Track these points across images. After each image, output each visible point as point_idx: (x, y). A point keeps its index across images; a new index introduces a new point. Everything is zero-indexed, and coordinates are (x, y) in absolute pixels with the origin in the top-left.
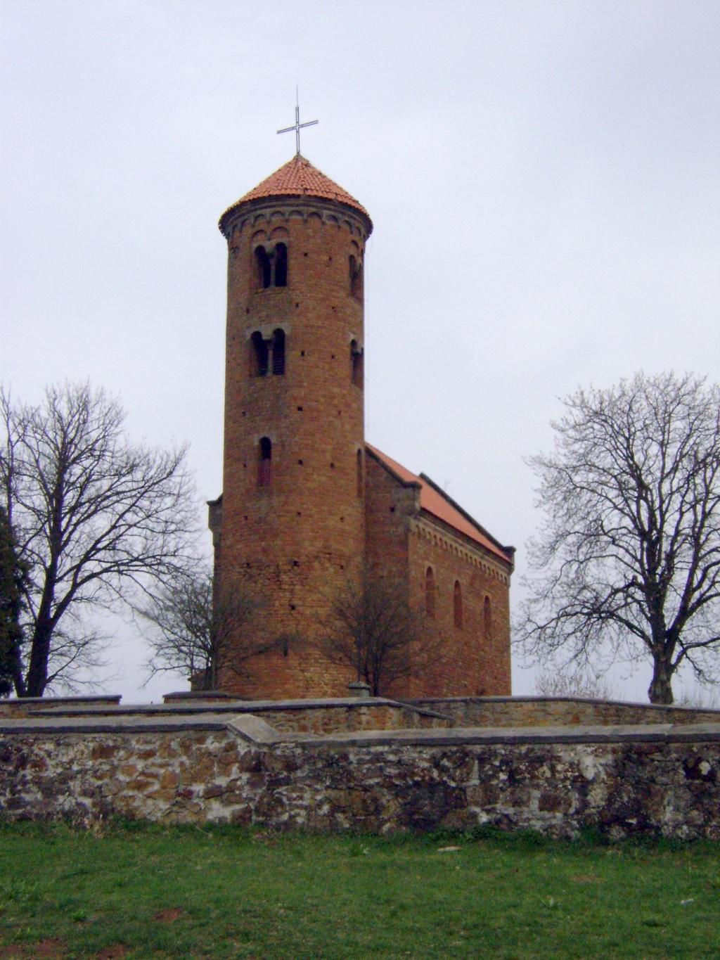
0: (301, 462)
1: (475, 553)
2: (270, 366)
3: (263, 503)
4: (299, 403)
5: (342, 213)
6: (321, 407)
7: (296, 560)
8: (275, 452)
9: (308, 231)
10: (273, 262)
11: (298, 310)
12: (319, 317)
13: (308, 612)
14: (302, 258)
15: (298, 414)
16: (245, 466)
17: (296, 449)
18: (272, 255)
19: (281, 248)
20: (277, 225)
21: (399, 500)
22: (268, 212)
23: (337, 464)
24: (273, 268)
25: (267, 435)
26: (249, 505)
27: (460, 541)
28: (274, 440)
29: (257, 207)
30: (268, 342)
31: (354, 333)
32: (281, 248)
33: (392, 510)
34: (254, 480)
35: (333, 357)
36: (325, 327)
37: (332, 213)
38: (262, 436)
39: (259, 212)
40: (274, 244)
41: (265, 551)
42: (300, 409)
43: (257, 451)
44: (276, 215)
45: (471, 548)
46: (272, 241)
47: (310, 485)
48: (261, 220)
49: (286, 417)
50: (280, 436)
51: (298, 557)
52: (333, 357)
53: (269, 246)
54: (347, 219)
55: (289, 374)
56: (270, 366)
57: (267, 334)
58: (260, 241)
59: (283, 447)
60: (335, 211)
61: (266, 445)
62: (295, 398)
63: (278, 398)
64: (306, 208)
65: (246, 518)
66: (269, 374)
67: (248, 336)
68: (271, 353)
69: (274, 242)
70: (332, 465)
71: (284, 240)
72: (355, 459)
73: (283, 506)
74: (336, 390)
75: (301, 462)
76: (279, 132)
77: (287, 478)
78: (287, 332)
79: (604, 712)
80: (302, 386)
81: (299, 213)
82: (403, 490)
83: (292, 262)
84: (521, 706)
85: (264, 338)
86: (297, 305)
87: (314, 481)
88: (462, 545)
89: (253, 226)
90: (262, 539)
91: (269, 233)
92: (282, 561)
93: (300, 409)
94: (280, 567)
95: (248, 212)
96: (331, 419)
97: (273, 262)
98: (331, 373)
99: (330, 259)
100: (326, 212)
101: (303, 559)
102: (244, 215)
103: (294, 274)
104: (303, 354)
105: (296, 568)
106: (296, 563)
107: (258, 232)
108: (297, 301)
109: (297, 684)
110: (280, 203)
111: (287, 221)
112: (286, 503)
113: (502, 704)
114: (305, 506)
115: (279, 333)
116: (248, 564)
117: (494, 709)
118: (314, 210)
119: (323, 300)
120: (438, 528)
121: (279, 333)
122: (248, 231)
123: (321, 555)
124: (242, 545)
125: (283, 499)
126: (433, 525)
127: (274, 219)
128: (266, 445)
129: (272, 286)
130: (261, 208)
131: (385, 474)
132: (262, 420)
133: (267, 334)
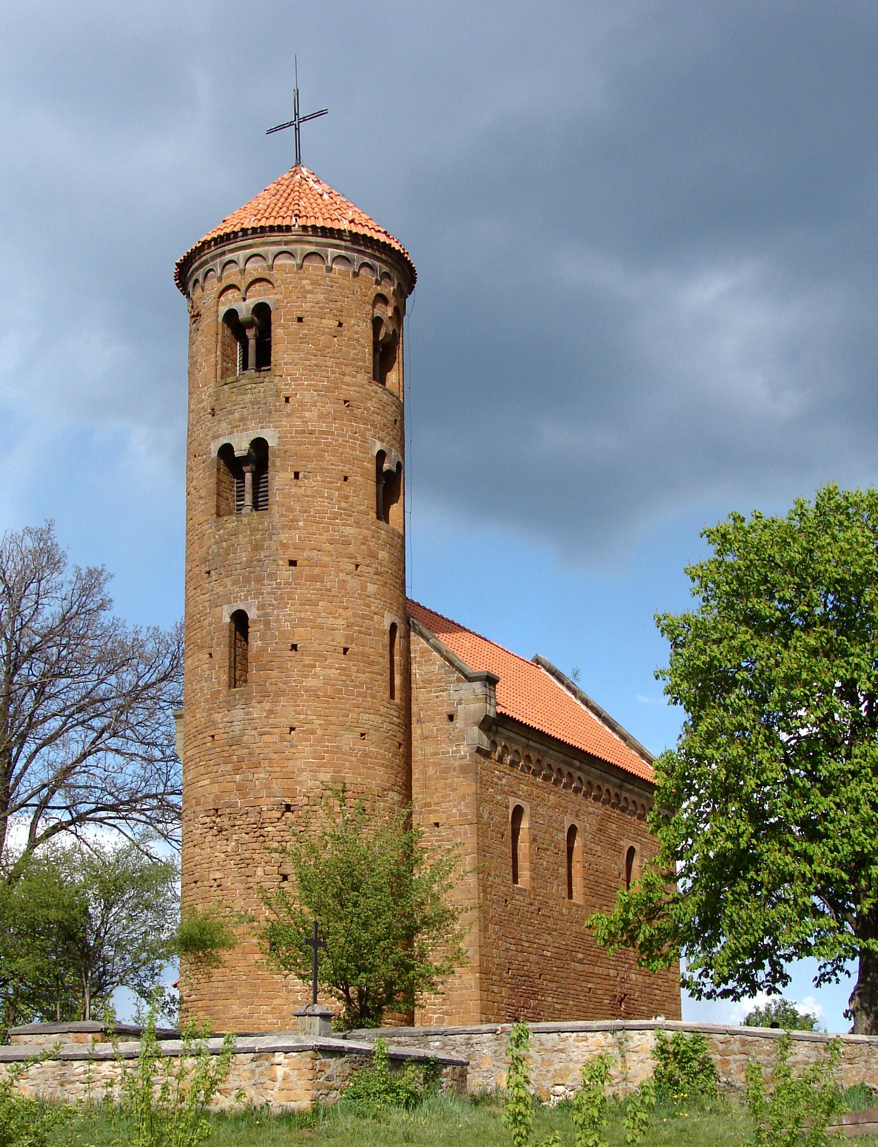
0: (294, 647)
1: (608, 782)
3: (238, 713)
4: (292, 554)
5: (358, 251)
6: (325, 559)
7: (288, 801)
8: (254, 631)
9: (304, 282)
10: (250, 333)
11: (289, 408)
12: (322, 417)
14: (295, 325)
15: (286, 573)
17: (287, 626)
18: (249, 324)
19: (262, 310)
20: (256, 275)
21: (459, 703)
22: (241, 255)
23: (353, 648)
24: (252, 342)
25: (242, 607)
26: (217, 717)
27: (577, 763)
28: (252, 614)
29: (226, 248)
31: (382, 441)
32: (262, 310)
33: (451, 718)
34: (225, 677)
35: (346, 479)
36: (332, 434)
37: (343, 252)
39: (228, 257)
40: (252, 306)
41: (241, 789)
42: (293, 563)
43: (227, 633)
45: (598, 772)
47: (310, 682)
48: (232, 269)
49: (272, 576)
50: (261, 607)
52: (346, 479)
53: (245, 310)
54: (367, 260)
55: (275, 509)
56: (248, 498)
57: (241, 447)
58: (231, 300)
59: (267, 623)
60: (346, 248)
61: (240, 620)
62: (284, 546)
63: (257, 547)
64: (298, 247)
66: (246, 510)
68: (248, 477)
69: (252, 302)
70: (346, 650)
72: (387, 640)
74: (349, 530)
75: (294, 647)
76: (270, 132)
77: (274, 673)
79: (721, 1047)
81: (291, 254)
82: (466, 685)
83: (278, 332)
84: (586, 1039)
85: (237, 454)
86: (287, 400)
87: (316, 676)
88: (580, 769)
89: (220, 279)
90: (237, 770)
91: (243, 289)
93: (293, 563)
95: (214, 258)
96: (342, 576)
97: (250, 333)
98: (344, 505)
99: (340, 325)
100: (331, 252)
101: (301, 800)
102: (206, 262)
103: (280, 351)
104: (297, 475)
105: (288, 814)
106: (288, 808)
108: (287, 394)
109: (292, 997)
111: (271, 268)
112: (271, 712)
113: (555, 1035)
114: (302, 717)
115: (259, 445)
117: (541, 1044)
118: (312, 249)
119: (328, 389)
120: (531, 743)
121: (259, 445)
122: (213, 286)
125: (267, 706)
126: (523, 740)
128: (240, 620)
129: (251, 372)
131: (440, 661)
132: (234, 583)
133: (241, 447)
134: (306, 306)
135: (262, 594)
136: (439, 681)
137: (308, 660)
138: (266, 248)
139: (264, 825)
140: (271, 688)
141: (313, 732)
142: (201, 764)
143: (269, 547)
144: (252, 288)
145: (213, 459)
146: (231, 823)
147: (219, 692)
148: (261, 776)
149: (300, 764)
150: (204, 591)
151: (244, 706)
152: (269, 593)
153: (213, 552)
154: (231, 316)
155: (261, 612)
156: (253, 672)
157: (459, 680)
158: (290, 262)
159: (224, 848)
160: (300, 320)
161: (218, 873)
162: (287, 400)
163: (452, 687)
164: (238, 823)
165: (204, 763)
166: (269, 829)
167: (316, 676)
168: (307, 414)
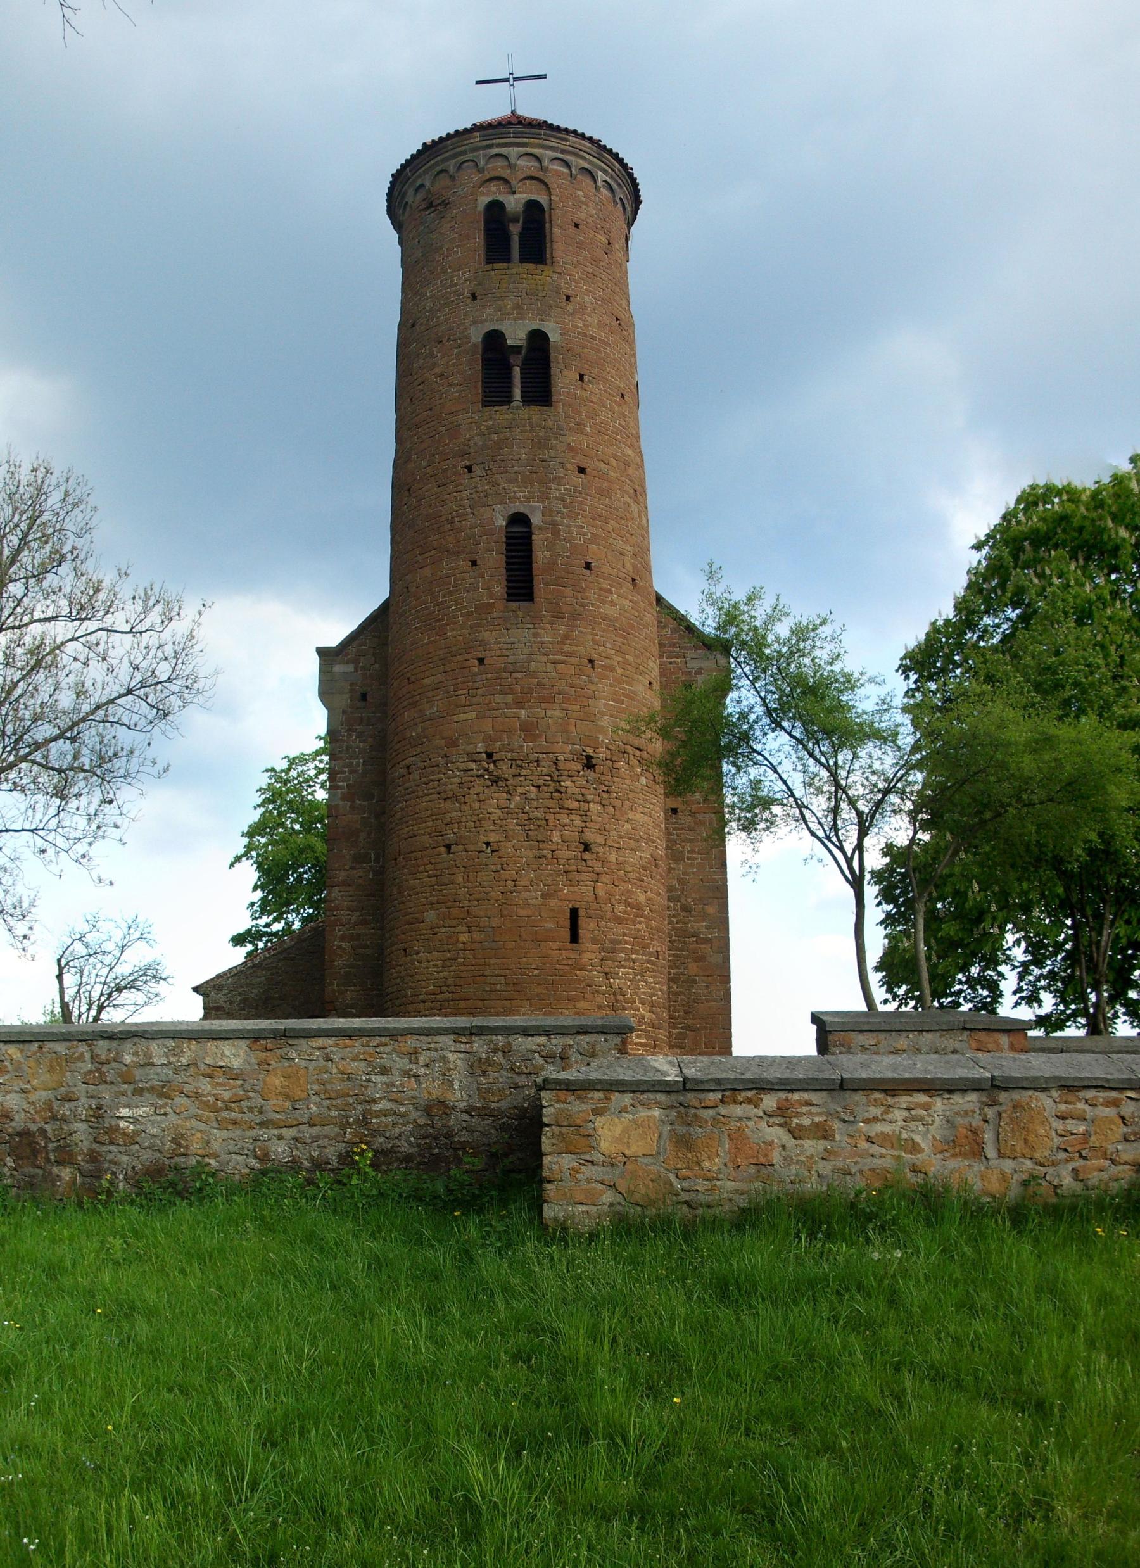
0: (588, 566)
2: (517, 393)
3: (521, 635)
7: (590, 751)
10: (515, 229)
11: (570, 307)
13: (613, 857)
14: (572, 229)
16: (474, 563)
20: (528, 173)
22: (512, 152)
24: (516, 239)
25: (522, 509)
28: (536, 519)
30: (517, 349)
32: (533, 207)
38: (513, 511)
39: (496, 151)
42: (582, 470)
44: (525, 158)
46: (517, 196)
49: (559, 480)
51: (595, 749)
53: (514, 202)
56: (517, 393)
57: (516, 334)
59: (556, 533)
63: (541, 444)
65: (481, 661)
67: (476, 335)
68: (517, 371)
71: (542, 199)
73: (562, 643)
77: (568, 590)
78: (554, 337)
80: (583, 433)
81: (567, 165)
86: (568, 298)
87: (613, 604)
90: (519, 705)
92: (564, 752)
93: (582, 470)
94: (561, 765)
97: (515, 229)
101: (602, 753)
102: (464, 153)
104: (581, 376)
107: (491, 179)
108: (568, 292)
110: (537, 141)
112: (566, 637)
116: (490, 755)
118: (586, 166)
121: (538, 338)
123: (629, 749)
124: (474, 715)
127: (522, 162)
130: (500, 145)
133: (516, 334)
134: (583, 216)
135: (549, 498)
136: (673, 645)
137: (605, 584)
138: (542, 151)
139: (560, 779)
140: (565, 608)
141: (613, 670)
142: (460, 692)
143: (554, 448)
144: (528, 182)
145: (475, 345)
146: (514, 771)
147: (490, 606)
148: (557, 713)
149: (600, 705)
150: (462, 488)
151: (532, 626)
152: (557, 498)
153: (476, 444)
154: (495, 209)
155: (549, 519)
156: (540, 587)
157: (696, 648)
158: (565, 170)
159: (503, 803)
160: (577, 226)
161: (493, 834)
162: (568, 298)
163: (689, 654)
164: (524, 772)
165: (466, 692)
166: (568, 783)
167: (613, 604)
168: (589, 319)
